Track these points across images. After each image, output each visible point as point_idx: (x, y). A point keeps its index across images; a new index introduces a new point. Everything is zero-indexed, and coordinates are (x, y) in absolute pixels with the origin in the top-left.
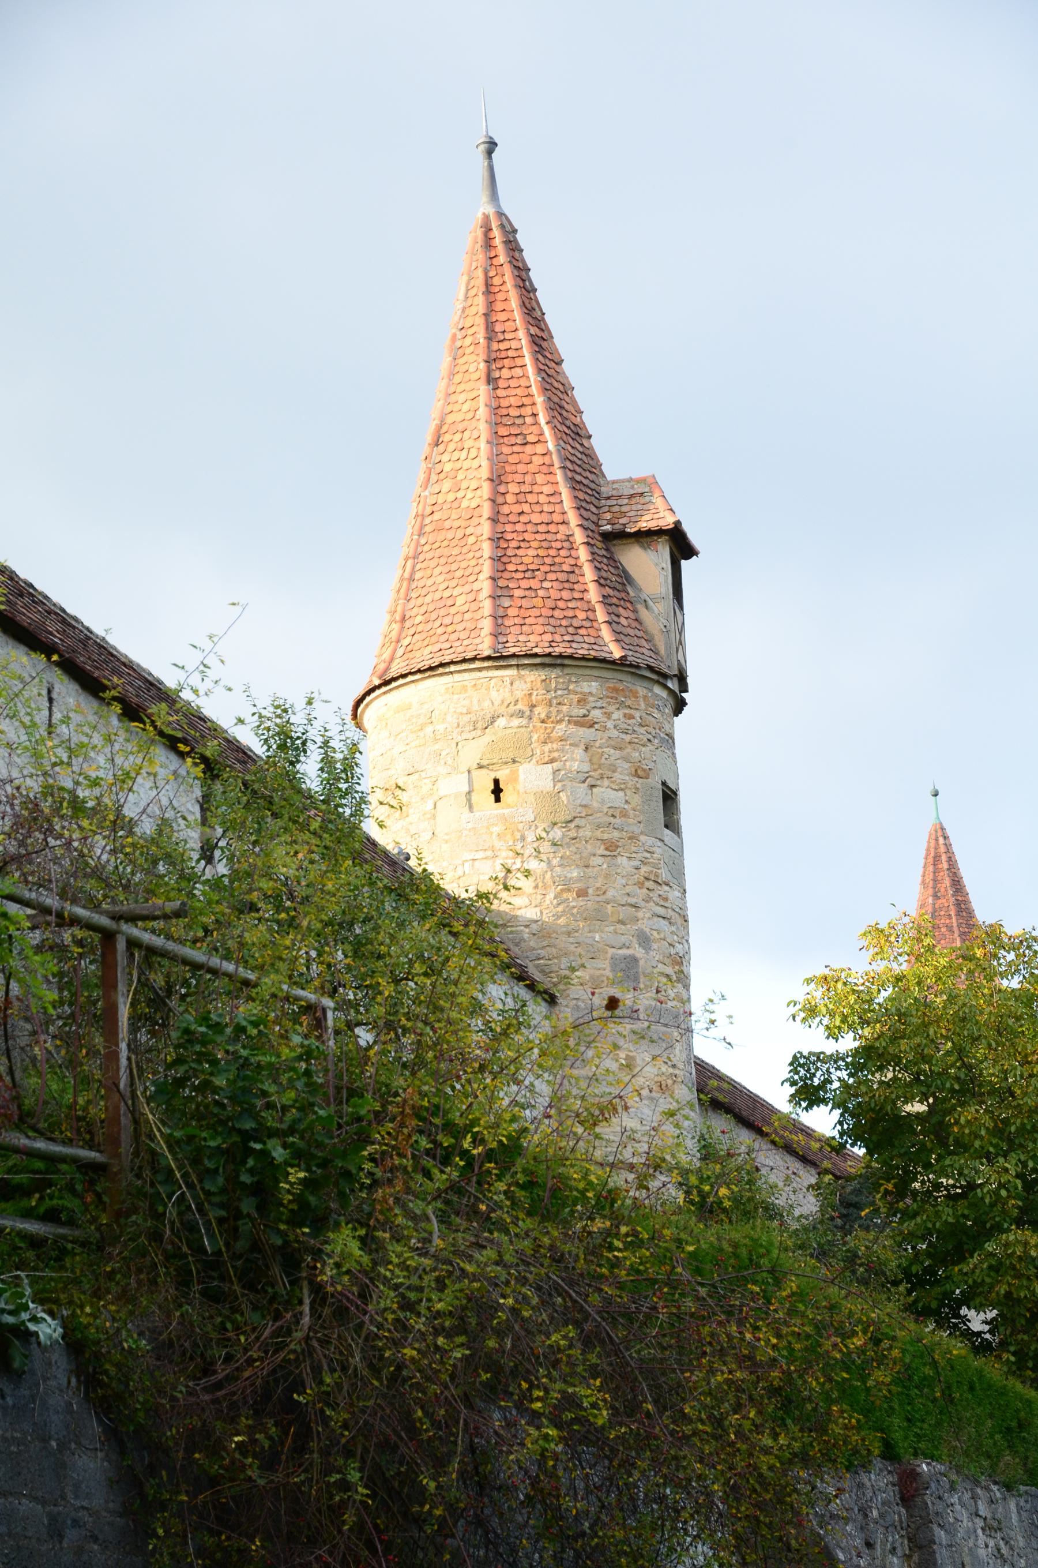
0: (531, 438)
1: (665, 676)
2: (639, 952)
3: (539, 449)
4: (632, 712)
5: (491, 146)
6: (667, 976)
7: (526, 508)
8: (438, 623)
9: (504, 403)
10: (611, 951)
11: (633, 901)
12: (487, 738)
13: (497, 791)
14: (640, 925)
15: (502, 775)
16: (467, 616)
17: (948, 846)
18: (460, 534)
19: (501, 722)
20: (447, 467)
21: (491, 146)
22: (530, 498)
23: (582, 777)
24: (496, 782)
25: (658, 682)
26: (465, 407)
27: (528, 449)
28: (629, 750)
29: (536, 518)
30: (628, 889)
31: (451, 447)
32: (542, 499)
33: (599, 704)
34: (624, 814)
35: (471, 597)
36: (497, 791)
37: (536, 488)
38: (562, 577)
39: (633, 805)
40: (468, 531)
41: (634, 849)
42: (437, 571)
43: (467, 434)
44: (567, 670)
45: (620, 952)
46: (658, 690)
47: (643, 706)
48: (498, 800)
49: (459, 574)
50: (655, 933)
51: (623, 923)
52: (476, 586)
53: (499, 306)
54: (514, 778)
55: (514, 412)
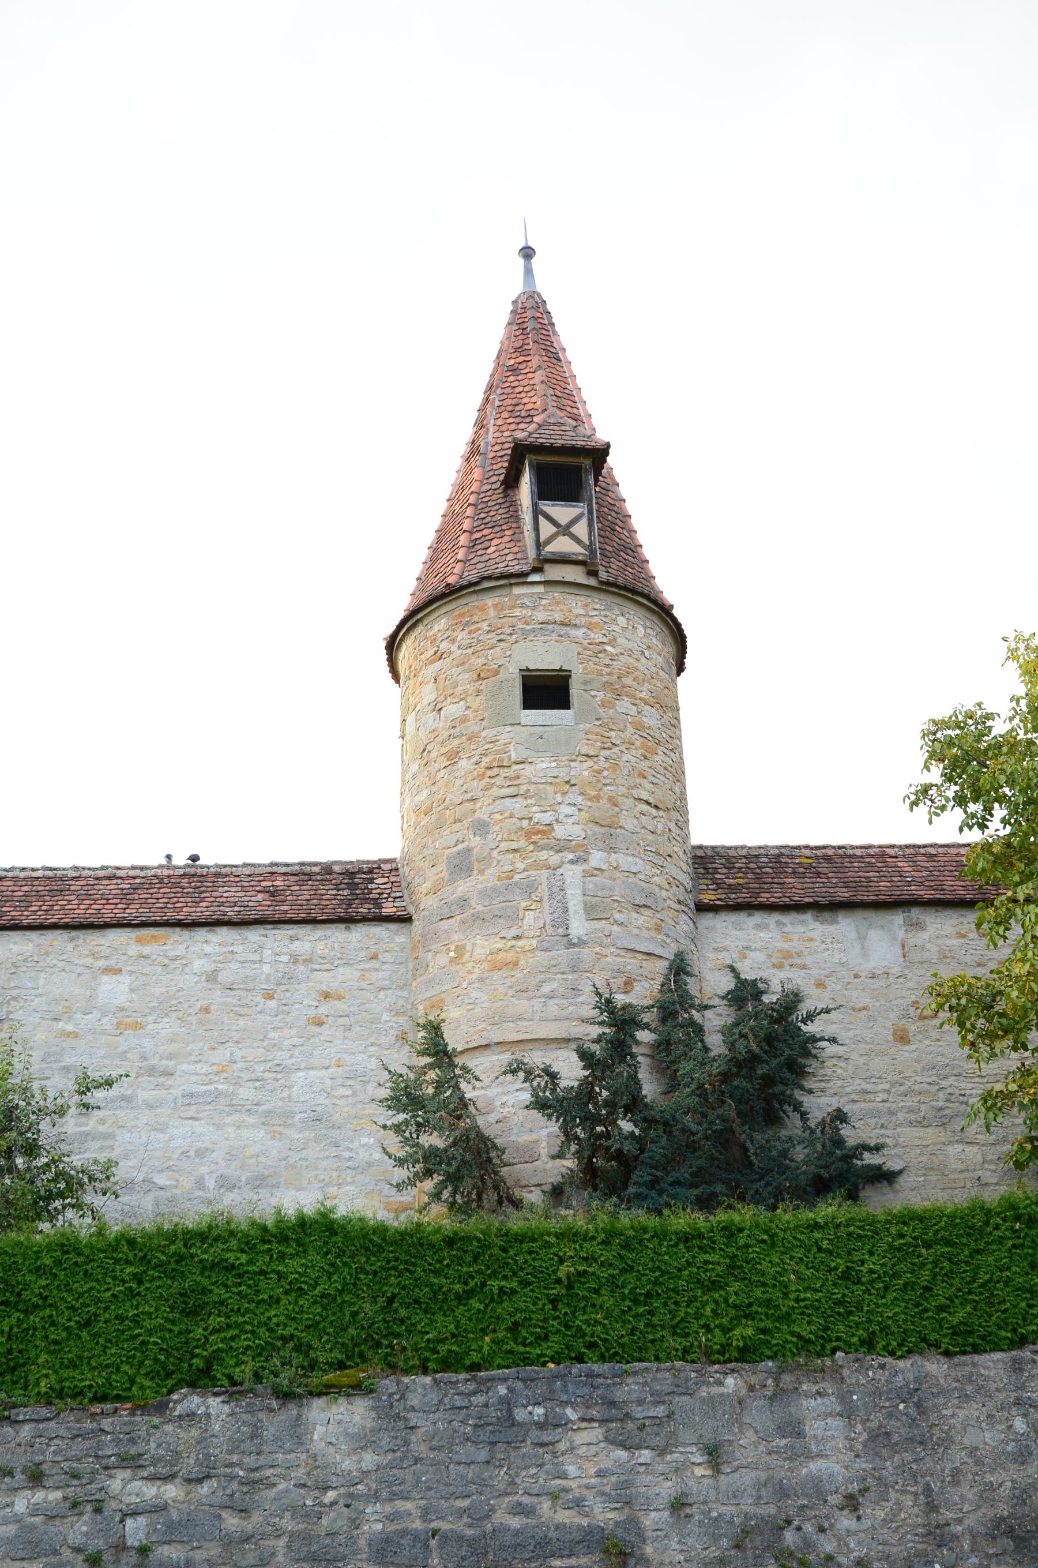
1: (524, 575)
2: (474, 841)
4: (478, 625)
5: (527, 253)
6: (515, 851)
10: (447, 852)
11: (469, 796)
14: (476, 815)
21: (527, 253)
23: (431, 707)
25: (511, 585)
28: (473, 659)
30: (464, 788)
33: (446, 636)
34: (464, 720)
39: (475, 706)
41: (473, 747)
44: (425, 622)
45: (455, 849)
46: (517, 591)
47: (492, 612)
50: (498, 816)
51: (460, 821)
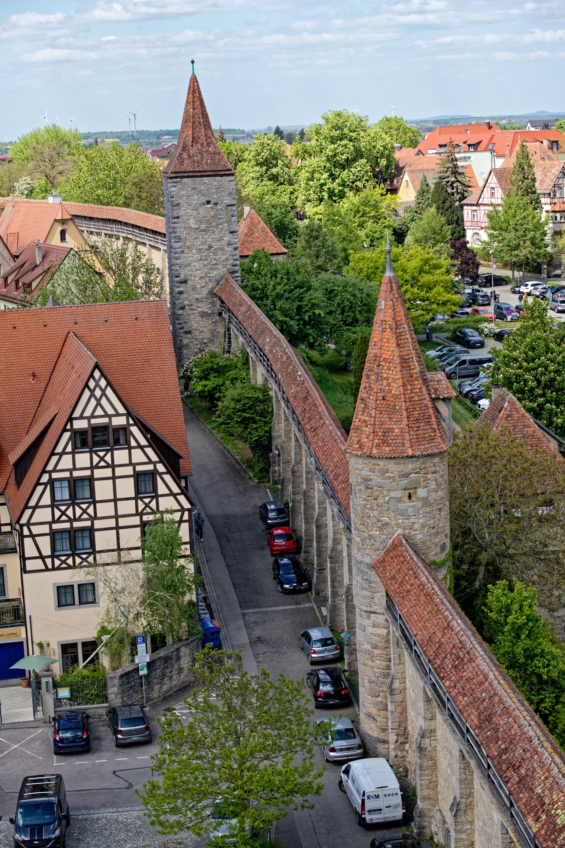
0: (412, 367)
3: (415, 371)
7: (413, 395)
8: (389, 438)
9: (403, 354)
12: (407, 481)
13: (410, 497)
15: (411, 491)
16: (400, 437)
17: (198, 86)
18: (392, 404)
19: (412, 475)
20: (385, 375)
22: (414, 391)
24: (410, 493)
26: (390, 353)
27: (412, 371)
29: (417, 398)
31: (385, 368)
32: (418, 390)
35: (400, 430)
36: (410, 497)
37: (416, 387)
38: (426, 420)
40: (396, 403)
42: (385, 416)
43: (391, 364)
48: (410, 499)
49: (394, 419)
52: (402, 426)
53: (397, 314)
54: (415, 493)
55: (407, 357)
